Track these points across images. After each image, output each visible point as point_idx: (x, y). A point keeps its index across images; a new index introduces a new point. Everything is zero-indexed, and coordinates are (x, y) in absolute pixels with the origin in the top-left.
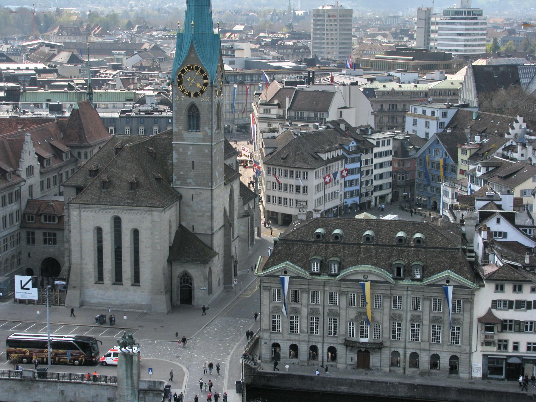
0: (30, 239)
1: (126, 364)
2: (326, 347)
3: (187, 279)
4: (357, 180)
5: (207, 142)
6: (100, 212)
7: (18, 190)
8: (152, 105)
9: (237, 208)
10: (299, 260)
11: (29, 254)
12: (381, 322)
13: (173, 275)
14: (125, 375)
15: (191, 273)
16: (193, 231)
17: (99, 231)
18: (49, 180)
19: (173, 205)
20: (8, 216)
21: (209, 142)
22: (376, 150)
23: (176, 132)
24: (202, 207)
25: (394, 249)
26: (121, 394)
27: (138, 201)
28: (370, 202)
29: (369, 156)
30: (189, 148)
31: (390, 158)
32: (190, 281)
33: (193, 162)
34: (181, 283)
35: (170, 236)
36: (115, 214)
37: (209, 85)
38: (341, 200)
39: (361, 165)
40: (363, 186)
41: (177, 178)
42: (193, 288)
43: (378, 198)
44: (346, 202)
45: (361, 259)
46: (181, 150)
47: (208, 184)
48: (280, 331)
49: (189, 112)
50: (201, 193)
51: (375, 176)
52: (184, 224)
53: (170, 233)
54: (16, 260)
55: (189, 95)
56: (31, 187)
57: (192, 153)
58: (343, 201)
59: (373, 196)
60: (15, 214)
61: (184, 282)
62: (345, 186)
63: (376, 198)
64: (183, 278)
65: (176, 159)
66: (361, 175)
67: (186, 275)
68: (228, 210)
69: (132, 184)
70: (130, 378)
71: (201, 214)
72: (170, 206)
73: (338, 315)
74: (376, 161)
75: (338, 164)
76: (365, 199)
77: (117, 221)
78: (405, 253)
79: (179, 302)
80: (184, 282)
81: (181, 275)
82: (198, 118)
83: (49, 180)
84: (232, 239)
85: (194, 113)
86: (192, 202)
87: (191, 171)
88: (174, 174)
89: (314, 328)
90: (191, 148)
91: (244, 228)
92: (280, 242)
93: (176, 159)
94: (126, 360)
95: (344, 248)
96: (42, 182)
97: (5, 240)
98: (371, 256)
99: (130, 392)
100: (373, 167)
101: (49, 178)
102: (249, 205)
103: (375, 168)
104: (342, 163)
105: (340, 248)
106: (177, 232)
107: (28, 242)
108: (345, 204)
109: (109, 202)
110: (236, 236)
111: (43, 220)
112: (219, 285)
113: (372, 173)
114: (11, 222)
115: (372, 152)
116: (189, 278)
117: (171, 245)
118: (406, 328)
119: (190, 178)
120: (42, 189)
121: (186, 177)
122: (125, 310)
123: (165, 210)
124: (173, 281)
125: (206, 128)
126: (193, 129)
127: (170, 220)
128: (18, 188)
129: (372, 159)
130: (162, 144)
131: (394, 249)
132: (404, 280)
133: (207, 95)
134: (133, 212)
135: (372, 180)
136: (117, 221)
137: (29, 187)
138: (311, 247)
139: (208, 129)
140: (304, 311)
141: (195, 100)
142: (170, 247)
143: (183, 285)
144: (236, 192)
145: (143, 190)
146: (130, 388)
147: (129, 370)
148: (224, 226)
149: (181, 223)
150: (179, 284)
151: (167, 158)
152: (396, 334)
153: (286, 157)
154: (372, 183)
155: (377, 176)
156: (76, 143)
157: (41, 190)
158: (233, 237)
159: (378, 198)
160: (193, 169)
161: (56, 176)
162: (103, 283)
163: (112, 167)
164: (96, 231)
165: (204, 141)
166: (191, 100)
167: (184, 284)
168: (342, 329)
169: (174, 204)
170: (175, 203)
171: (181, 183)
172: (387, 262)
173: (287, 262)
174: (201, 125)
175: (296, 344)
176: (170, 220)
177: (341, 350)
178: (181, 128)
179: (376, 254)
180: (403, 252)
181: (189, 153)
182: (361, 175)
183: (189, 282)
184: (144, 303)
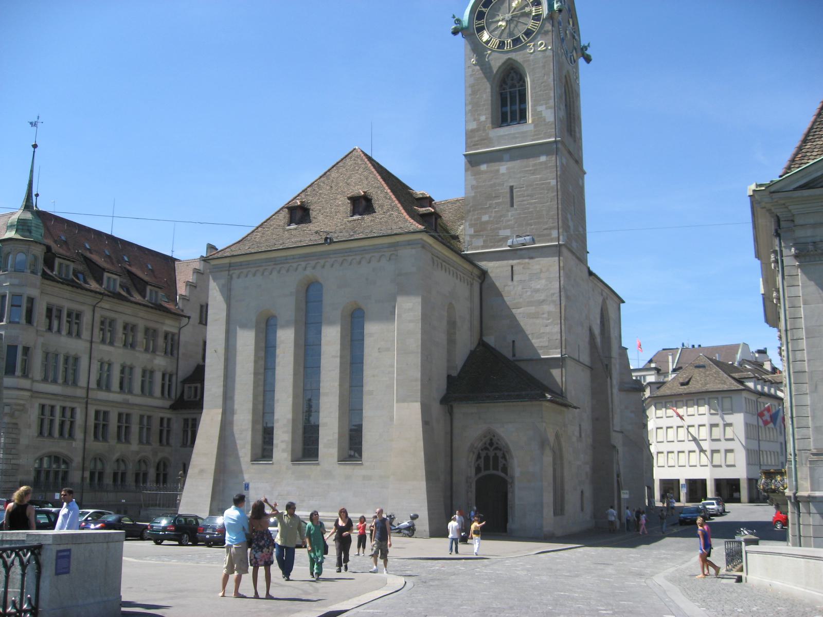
3: (496, 458)
6: (275, 273)
13: (455, 444)
16: (514, 355)
23: (473, 131)
24: (537, 291)
32: (501, 462)
33: (512, 188)
34: (478, 469)
36: (309, 272)
41: (475, 232)
42: (509, 480)
47: (550, 235)
49: (501, 86)
52: (490, 340)
53: (451, 341)
61: (487, 468)
64: (483, 454)
67: (491, 444)
68: (598, 340)
80: (487, 468)
81: (480, 445)
85: (513, 86)
86: (510, 283)
87: (508, 211)
112: (582, 510)
116: (499, 454)
117: (455, 373)
119: (505, 228)
126: (511, 122)
134: (350, 258)
139: (547, 108)
142: (449, 377)
143: (483, 473)
149: (485, 339)
160: (512, 205)
167: (487, 472)
171: (484, 241)
178: (483, 118)
183: (500, 466)
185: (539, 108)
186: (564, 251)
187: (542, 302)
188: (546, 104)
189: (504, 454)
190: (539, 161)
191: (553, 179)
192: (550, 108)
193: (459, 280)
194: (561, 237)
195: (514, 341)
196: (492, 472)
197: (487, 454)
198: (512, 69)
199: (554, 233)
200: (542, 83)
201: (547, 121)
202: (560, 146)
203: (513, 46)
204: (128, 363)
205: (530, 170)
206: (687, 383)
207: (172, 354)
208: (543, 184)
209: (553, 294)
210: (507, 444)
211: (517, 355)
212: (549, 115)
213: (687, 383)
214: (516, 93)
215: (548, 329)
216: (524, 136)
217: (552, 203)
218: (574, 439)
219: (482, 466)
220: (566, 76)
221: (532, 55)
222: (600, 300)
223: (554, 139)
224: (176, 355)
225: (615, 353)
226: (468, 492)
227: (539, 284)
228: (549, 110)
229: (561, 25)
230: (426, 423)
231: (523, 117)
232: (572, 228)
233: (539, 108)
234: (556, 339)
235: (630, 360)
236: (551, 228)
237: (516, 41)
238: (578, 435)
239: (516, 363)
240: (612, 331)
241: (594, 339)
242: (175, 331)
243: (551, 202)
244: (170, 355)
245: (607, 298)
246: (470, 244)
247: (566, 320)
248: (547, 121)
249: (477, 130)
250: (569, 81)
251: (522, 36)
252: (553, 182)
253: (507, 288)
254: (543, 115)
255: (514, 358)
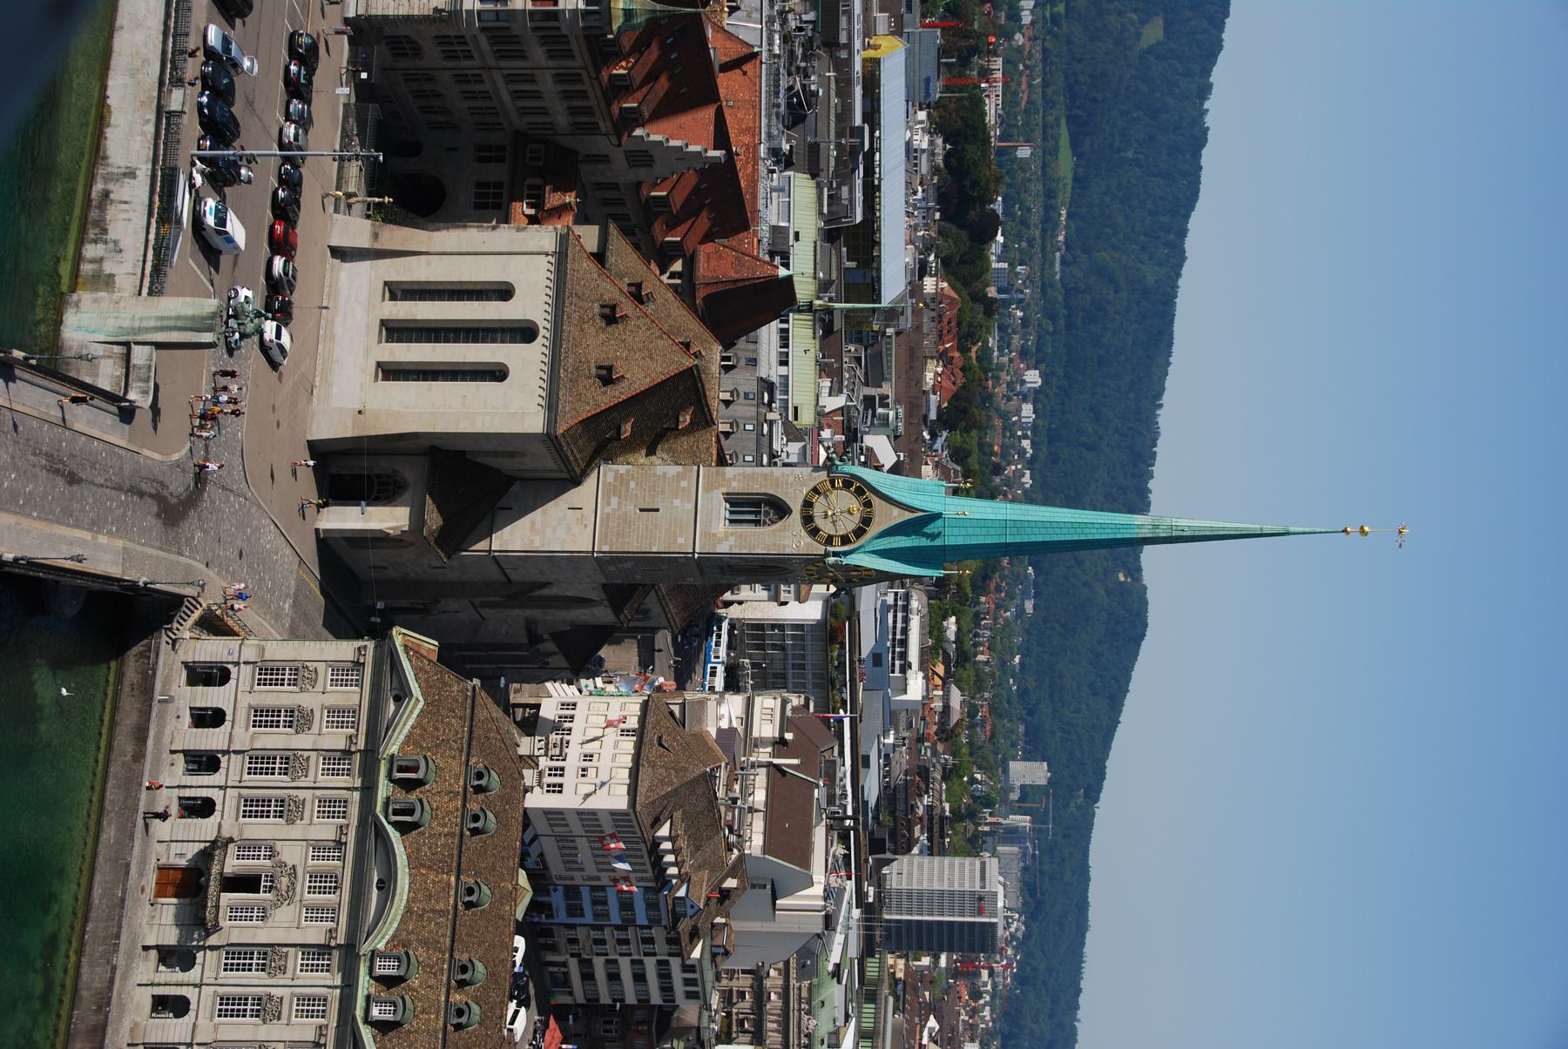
0: (487, 154)
1: (193, 318)
2: (216, 795)
4: (606, 915)
5: (700, 542)
7: (599, 129)
8: (784, 455)
9: (550, 617)
10: (426, 730)
11: (455, 149)
12: (269, 924)
14: (166, 314)
17: (504, 292)
18: (621, 202)
19: (560, 462)
20: (541, 104)
21: (701, 547)
22: (675, 963)
23: (725, 473)
24: (554, 531)
25: (443, 953)
26: (122, 304)
27: (571, 381)
28: (554, 948)
29: (661, 947)
30: (689, 501)
31: (656, 998)
33: (657, 510)
34: (378, 476)
35: (487, 453)
36: (542, 332)
37: (830, 549)
38: (561, 878)
39: (642, 927)
40: (592, 933)
43: (563, 970)
44: (555, 890)
45: (423, 875)
46: (684, 484)
47: (606, 544)
48: (259, 684)
50: (586, 526)
51: (615, 962)
52: (516, 488)
53: (496, 454)
54: (442, 118)
55: (808, 504)
56: (605, 159)
57: (677, 507)
58: (558, 882)
59: (568, 957)
60: (546, 119)
62: (593, 888)
63: (564, 964)
65: (665, 474)
66: (617, 927)
67: (399, 488)
68: (546, 592)
69: (610, 369)
70: (159, 324)
71: (538, 526)
72: (557, 457)
73: (290, 822)
74: (650, 964)
75: (646, 872)
76: (561, 937)
77: (524, 332)
78: (432, 982)
79: (333, 470)
82: (757, 523)
83: (621, 202)
84: (477, 600)
85: (767, 514)
87: (635, 506)
88: (630, 467)
89: (261, 762)
90: (691, 506)
91: (504, 632)
92: (470, 688)
93: (665, 474)
94: (203, 318)
95: (452, 835)
96: (615, 186)
97: (486, 96)
98: (430, 899)
99: (126, 324)
100: (635, 957)
101: (624, 204)
102: (554, 653)
103: (633, 962)
104: (645, 880)
105: (451, 827)
106: (497, 471)
107: (481, 148)
108: (551, 888)
109: (568, 318)
110: (486, 612)
111: (530, 181)
113: (621, 955)
114: (523, 112)
115: (670, 955)
117: (468, 456)
118: (252, 981)
120: (601, 186)
121: (623, 493)
122: (320, 347)
123: (548, 442)
125: (732, 540)
127: (523, 455)
128: (603, 129)
129: (654, 954)
130: (698, 447)
131: (443, 953)
132: (368, 978)
133: (808, 544)
135: (606, 954)
136: (524, 332)
137: (607, 156)
138: (454, 758)
139: (731, 547)
140: (303, 741)
141: (796, 516)
142: (464, 452)
144: (585, 615)
145: (594, 394)
146: (136, 325)
147: (179, 324)
148: (509, 581)
149: (518, 482)
151: (665, 457)
152: (239, 956)
153: (663, 747)
154: (598, 954)
155: (615, 966)
156: (701, 270)
157: (598, 184)
158: (484, 605)
159: (563, 970)
160: (641, 510)
161: (629, 220)
162: (383, 300)
163: (649, 329)
164: (504, 287)
165: (706, 534)
166: (796, 507)
168: (258, 829)
169: (562, 465)
170: (564, 469)
172: (412, 937)
173: (422, 703)
174: (739, 529)
175: (231, 681)
176: (523, 455)
177: (205, 829)
178: (734, 484)
179: (434, 911)
180: (435, 974)
181: (677, 502)
182: (617, 927)
184: (335, 390)
188: (736, 546)
192: (730, 549)
199: (606, 548)
206: (660, 745)
212: (723, 548)
213: (660, 745)
231: (731, 521)
236: (611, 546)
246: (611, 470)
249: (724, 480)
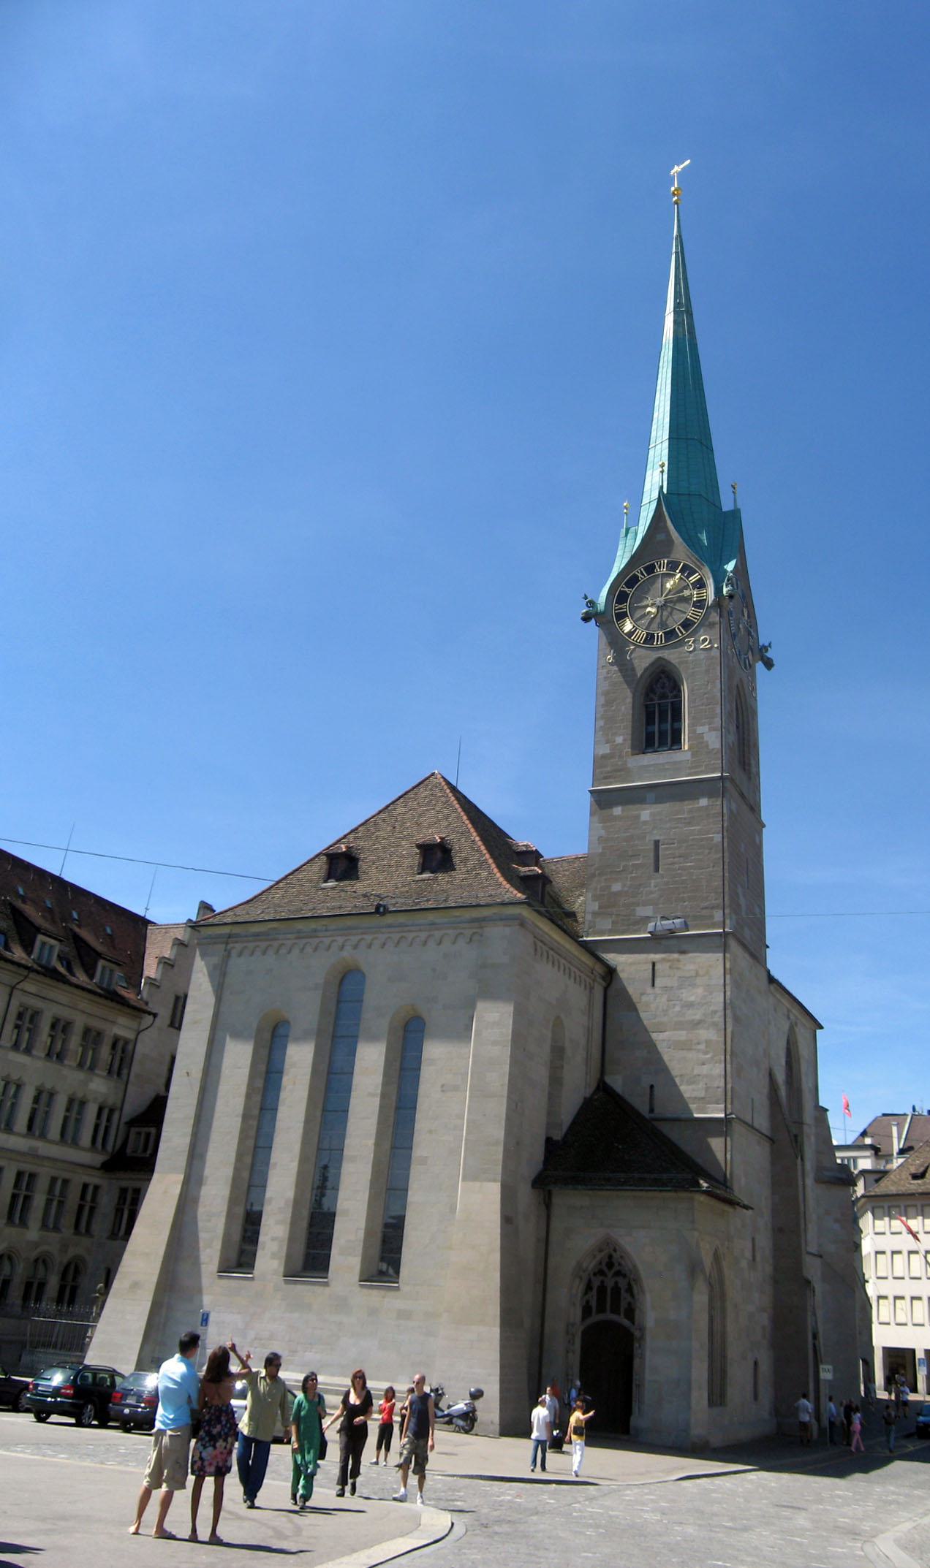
3: (616, 1290)
15: (628, 1248)
16: (652, 1110)
24: (690, 1005)
34: (587, 1311)
47: (712, 917)
61: (601, 1309)
64: (596, 1283)
67: (610, 1265)
68: (783, 1092)
80: (601, 1309)
81: (591, 1265)
116: (622, 1283)
124: (549, 1296)
139: (711, 729)
143: (596, 1318)
150: (578, 1312)
167: (601, 1317)
183: (623, 1305)
185: (700, 730)
186: (733, 944)
187: (696, 1024)
189: (629, 1284)
190: (697, 806)
191: (718, 833)
192: (714, 729)
193: (572, 979)
194: (728, 922)
195: (652, 1087)
196: (609, 1316)
197: (602, 1282)
198: (663, 672)
199: (718, 915)
200: (706, 694)
201: (711, 747)
202: (728, 784)
203: (665, 642)
204: (48, 1086)
205: (685, 819)
207: (119, 1074)
208: (702, 840)
209: (715, 1012)
210: (635, 1266)
211: (656, 1111)
212: (713, 740)
214: (668, 706)
215: (705, 1070)
216: (677, 767)
217: (715, 869)
218: (744, 1264)
219: (594, 1304)
220: (737, 686)
221: (692, 655)
222: (786, 1027)
223: (720, 775)
224: (125, 1077)
225: (808, 1116)
226: (568, 1352)
227: (693, 995)
228: (714, 732)
229: (732, 616)
230: (507, 1220)
232: (744, 908)
233: (700, 730)
234: (718, 1087)
235: (831, 1130)
237: (670, 634)
238: (751, 1258)
239: (656, 1123)
240: (804, 1079)
241: (776, 1090)
242: (130, 1035)
243: (713, 866)
244: (115, 1077)
245: (796, 1024)
247: (733, 1055)
248: (711, 747)
250: (742, 694)
251: (678, 628)
252: (718, 838)
253: (644, 998)
254: (705, 739)
255: (652, 1115)
